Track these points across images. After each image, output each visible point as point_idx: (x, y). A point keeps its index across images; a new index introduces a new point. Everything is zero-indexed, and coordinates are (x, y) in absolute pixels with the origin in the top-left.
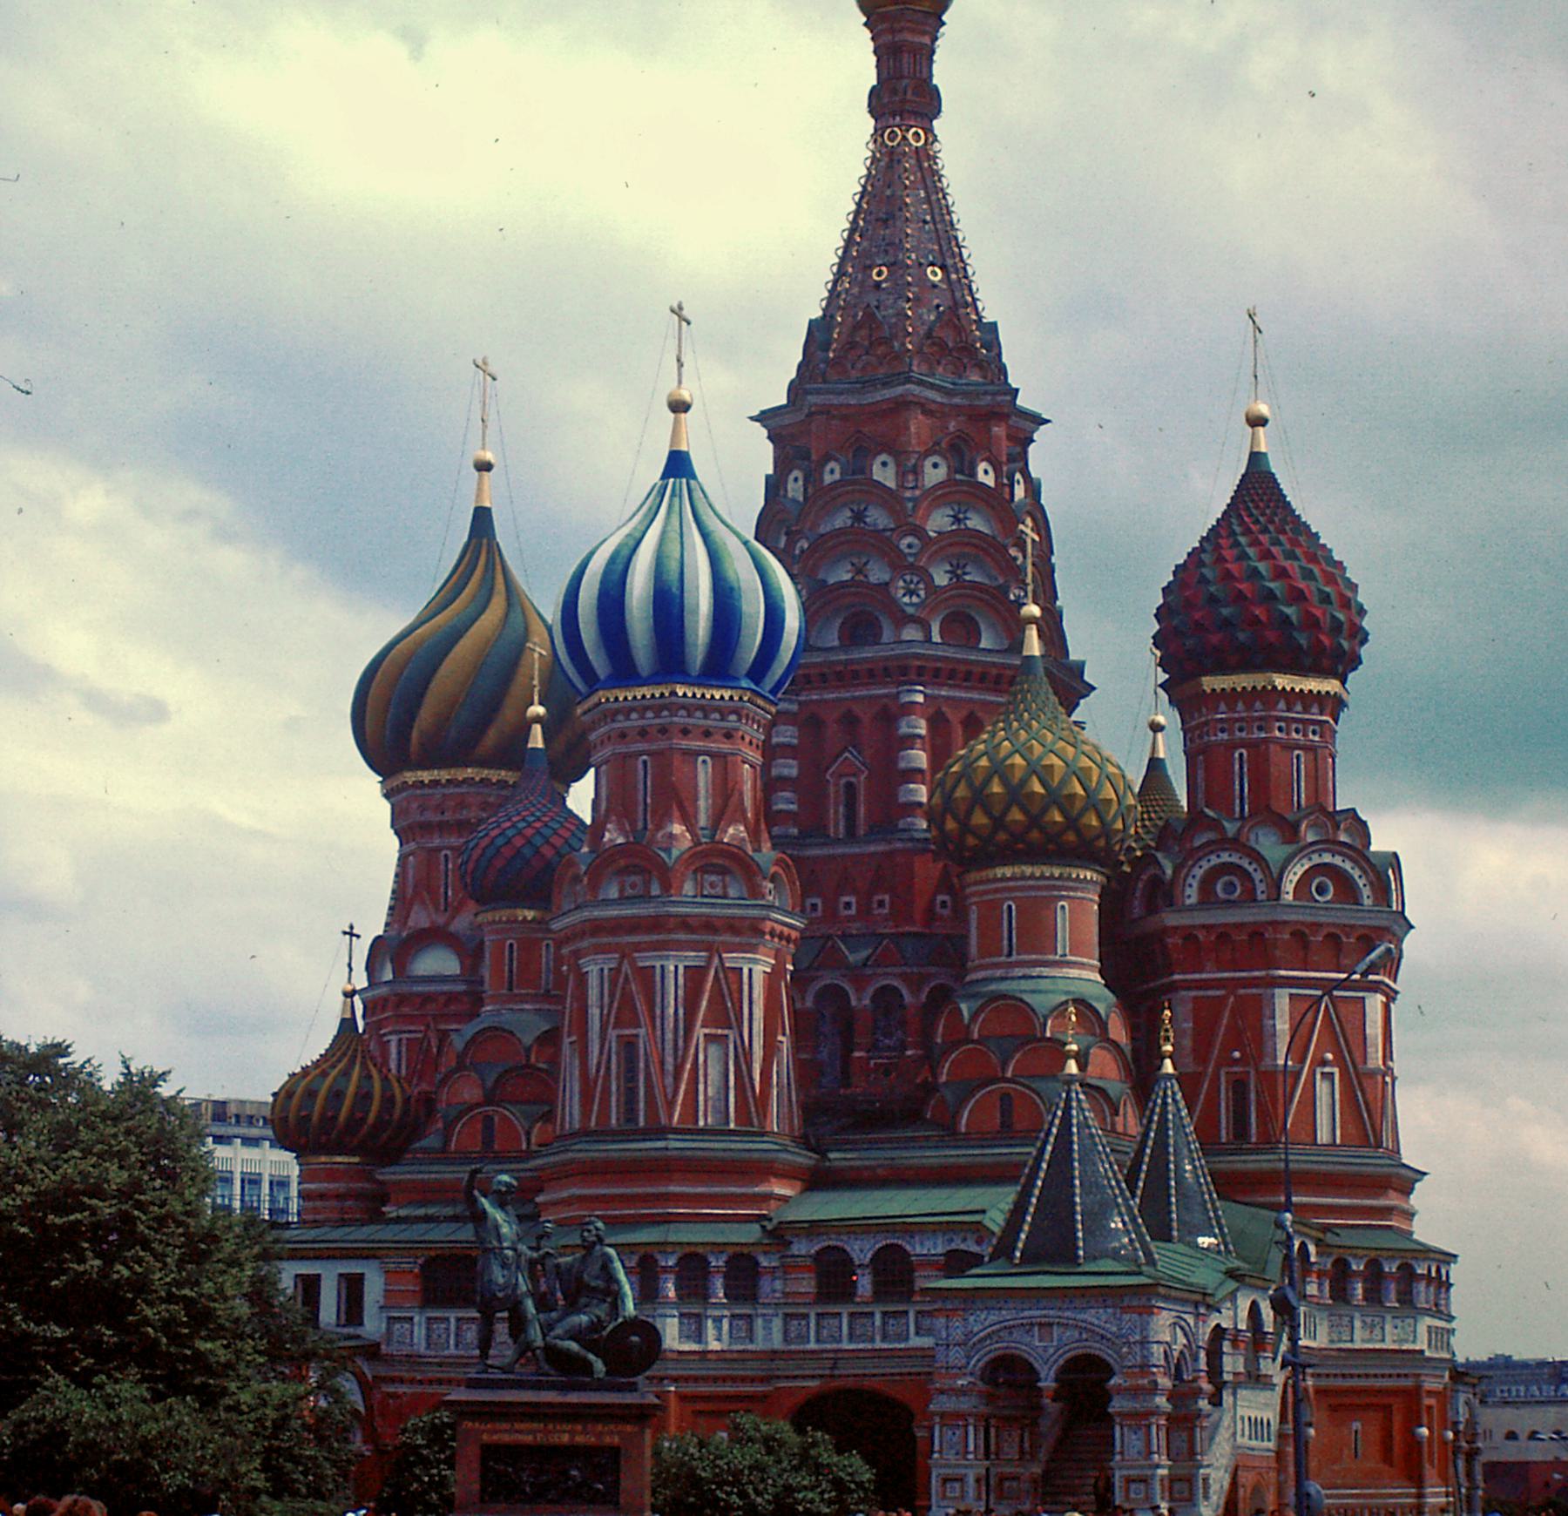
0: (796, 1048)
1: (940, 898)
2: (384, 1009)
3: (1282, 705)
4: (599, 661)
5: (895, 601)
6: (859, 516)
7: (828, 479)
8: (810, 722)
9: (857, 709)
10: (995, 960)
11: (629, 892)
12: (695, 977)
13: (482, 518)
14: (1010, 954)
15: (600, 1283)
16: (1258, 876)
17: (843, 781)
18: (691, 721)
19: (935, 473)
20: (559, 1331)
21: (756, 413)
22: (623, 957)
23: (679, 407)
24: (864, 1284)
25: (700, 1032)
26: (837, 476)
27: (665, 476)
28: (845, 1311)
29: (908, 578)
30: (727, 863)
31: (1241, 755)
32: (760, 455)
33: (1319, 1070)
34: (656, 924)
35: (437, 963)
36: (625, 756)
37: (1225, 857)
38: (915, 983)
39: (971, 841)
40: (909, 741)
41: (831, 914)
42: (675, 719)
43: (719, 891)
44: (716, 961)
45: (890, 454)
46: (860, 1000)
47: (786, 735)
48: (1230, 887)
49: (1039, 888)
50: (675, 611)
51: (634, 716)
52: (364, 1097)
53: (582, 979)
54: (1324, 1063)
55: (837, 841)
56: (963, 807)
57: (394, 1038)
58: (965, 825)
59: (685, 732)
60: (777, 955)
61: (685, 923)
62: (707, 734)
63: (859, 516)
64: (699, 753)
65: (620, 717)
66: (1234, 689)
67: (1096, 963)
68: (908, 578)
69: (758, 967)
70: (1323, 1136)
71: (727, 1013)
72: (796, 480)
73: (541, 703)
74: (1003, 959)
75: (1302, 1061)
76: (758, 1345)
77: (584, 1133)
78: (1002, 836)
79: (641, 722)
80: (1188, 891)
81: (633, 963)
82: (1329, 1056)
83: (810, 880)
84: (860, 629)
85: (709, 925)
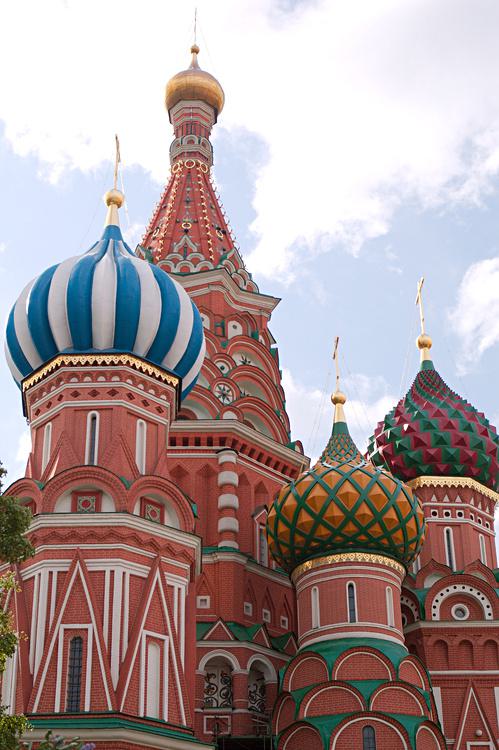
9: (187, 467)
23: (114, 202)
25: (143, 633)
29: (222, 386)
31: (448, 532)
34: (112, 534)
36: (77, 410)
38: (244, 656)
39: (323, 531)
44: (158, 575)
56: (319, 505)
58: (319, 520)
59: (131, 396)
61: (135, 537)
62: (145, 403)
66: (446, 486)
68: (222, 386)
74: (348, 624)
78: (351, 528)
80: (433, 611)
85: (152, 543)
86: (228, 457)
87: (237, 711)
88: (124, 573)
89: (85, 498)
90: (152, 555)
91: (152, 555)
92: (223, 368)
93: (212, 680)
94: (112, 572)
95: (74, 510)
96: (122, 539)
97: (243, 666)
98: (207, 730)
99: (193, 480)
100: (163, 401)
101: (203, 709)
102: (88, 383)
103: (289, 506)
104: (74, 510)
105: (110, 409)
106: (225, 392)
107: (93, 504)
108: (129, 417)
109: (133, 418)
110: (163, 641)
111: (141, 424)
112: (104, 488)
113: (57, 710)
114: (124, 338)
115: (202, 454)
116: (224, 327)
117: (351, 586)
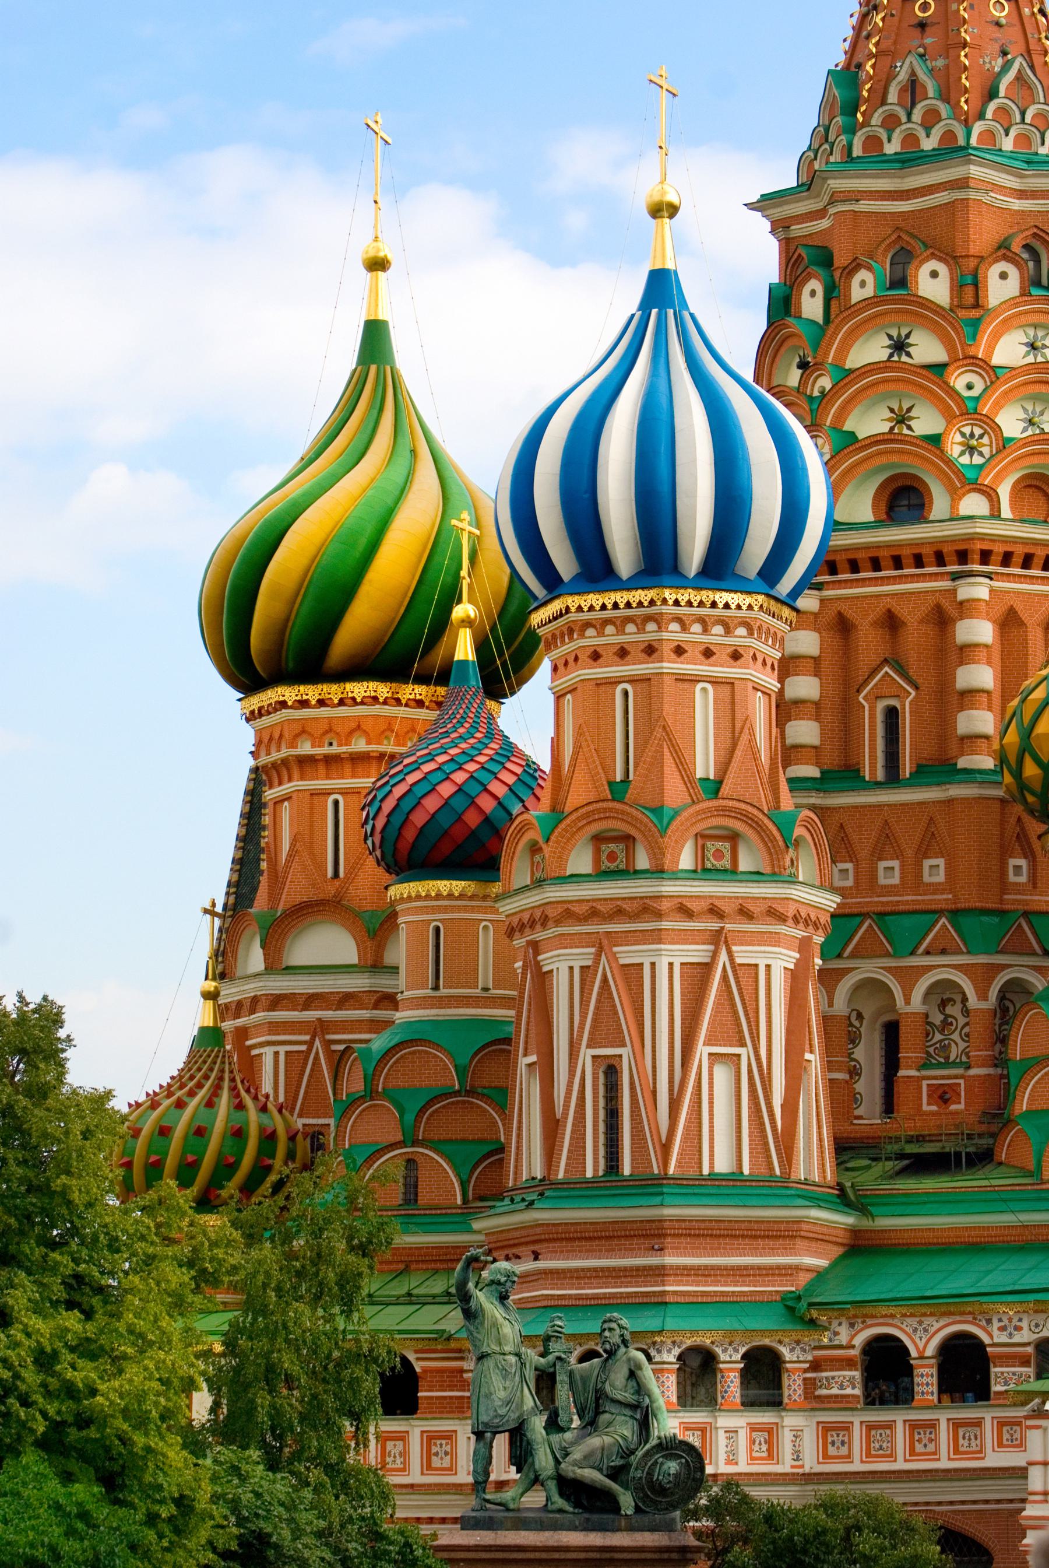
0: (830, 1066)
1: (1013, 862)
2: (252, 1011)
4: (563, 560)
5: (949, 462)
6: (900, 346)
7: (857, 294)
8: (840, 627)
9: (902, 611)
11: (606, 865)
12: (698, 976)
13: (375, 338)
15: (628, 1396)
17: (881, 705)
19: (1002, 285)
20: (577, 1454)
21: (755, 198)
22: (600, 949)
24: (926, 1380)
25: (702, 1051)
26: (869, 292)
27: (646, 305)
28: (899, 1417)
30: (738, 826)
32: (762, 258)
34: (647, 908)
35: (328, 945)
36: (600, 683)
38: (983, 976)
40: (966, 653)
41: (867, 881)
42: (665, 635)
43: (726, 862)
44: (723, 957)
45: (940, 259)
46: (913, 1002)
47: (807, 642)
50: (665, 488)
52: (239, 1133)
53: (543, 979)
55: (878, 784)
57: (268, 1052)
59: (679, 651)
60: (804, 946)
62: (708, 653)
63: (900, 346)
64: (695, 680)
65: (590, 632)
68: (967, 430)
69: (776, 961)
71: (739, 1026)
72: (813, 293)
73: (470, 602)
76: (785, 1467)
77: (545, 1186)
79: (622, 639)
83: (840, 841)
84: (903, 498)
87: (973, 1072)
88: (671, 964)
89: (612, 846)
90: (715, 925)
91: (715, 925)
92: (970, 387)
93: (949, 1010)
94: (653, 964)
97: (983, 996)
98: (929, 1104)
99: (916, 636)
101: (919, 1070)
102: (611, 637)
103: (1010, 744)
105: (646, 679)
106: (974, 442)
107: (622, 856)
108: (679, 684)
109: (686, 685)
110: (739, 1056)
111: (704, 690)
112: (633, 832)
113: (589, 1174)
114: (659, 558)
115: (928, 584)
116: (977, 285)
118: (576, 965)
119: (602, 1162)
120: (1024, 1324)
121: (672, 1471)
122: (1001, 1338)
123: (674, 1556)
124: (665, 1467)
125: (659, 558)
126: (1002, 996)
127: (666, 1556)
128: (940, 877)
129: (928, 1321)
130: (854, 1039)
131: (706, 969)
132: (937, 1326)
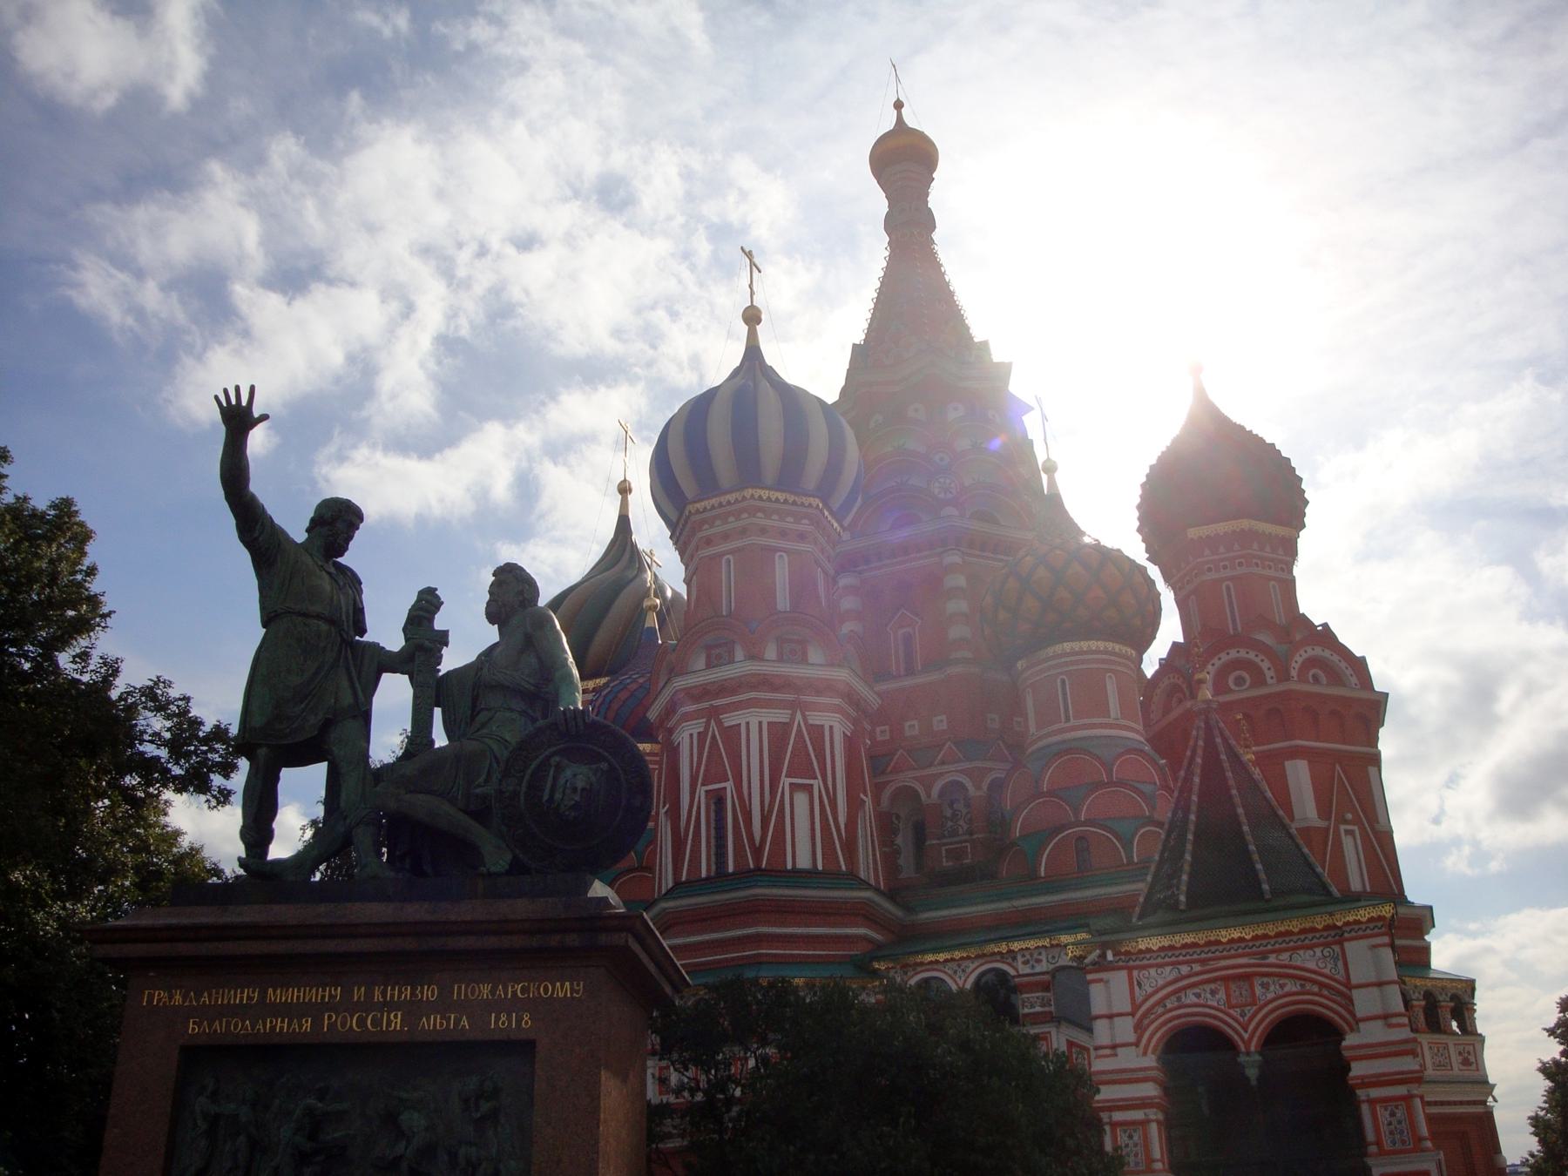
3: (1255, 546)
10: (1056, 726)
14: (1068, 720)
16: (1265, 665)
17: (901, 631)
18: (768, 522)
25: (785, 781)
33: (1343, 827)
37: (1233, 654)
42: (754, 520)
44: (799, 716)
48: (1239, 681)
49: (1083, 662)
51: (718, 522)
54: (1346, 822)
60: (855, 722)
62: (783, 534)
67: (1140, 728)
70: (1356, 885)
74: (1063, 725)
75: (1329, 819)
81: (719, 723)
82: (1349, 816)
86: (954, 558)
95: (709, 666)
96: (753, 687)
97: (978, 788)
100: (804, 526)
104: (709, 666)
113: (704, 875)
117: (1063, 682)
118: (695, 732)
119: (713, 867)
120: (1043, 957)
121: (580, 784)
122: (1028, 971)
123: (573, 940)
124: (568, 773)
125: (749, 471)
126: (990, 787)
127: (554, 941)
128: (944, 726)
129: (964, 964)
130: (895, 832)
131: (787, 726)
132: (972, 966)
